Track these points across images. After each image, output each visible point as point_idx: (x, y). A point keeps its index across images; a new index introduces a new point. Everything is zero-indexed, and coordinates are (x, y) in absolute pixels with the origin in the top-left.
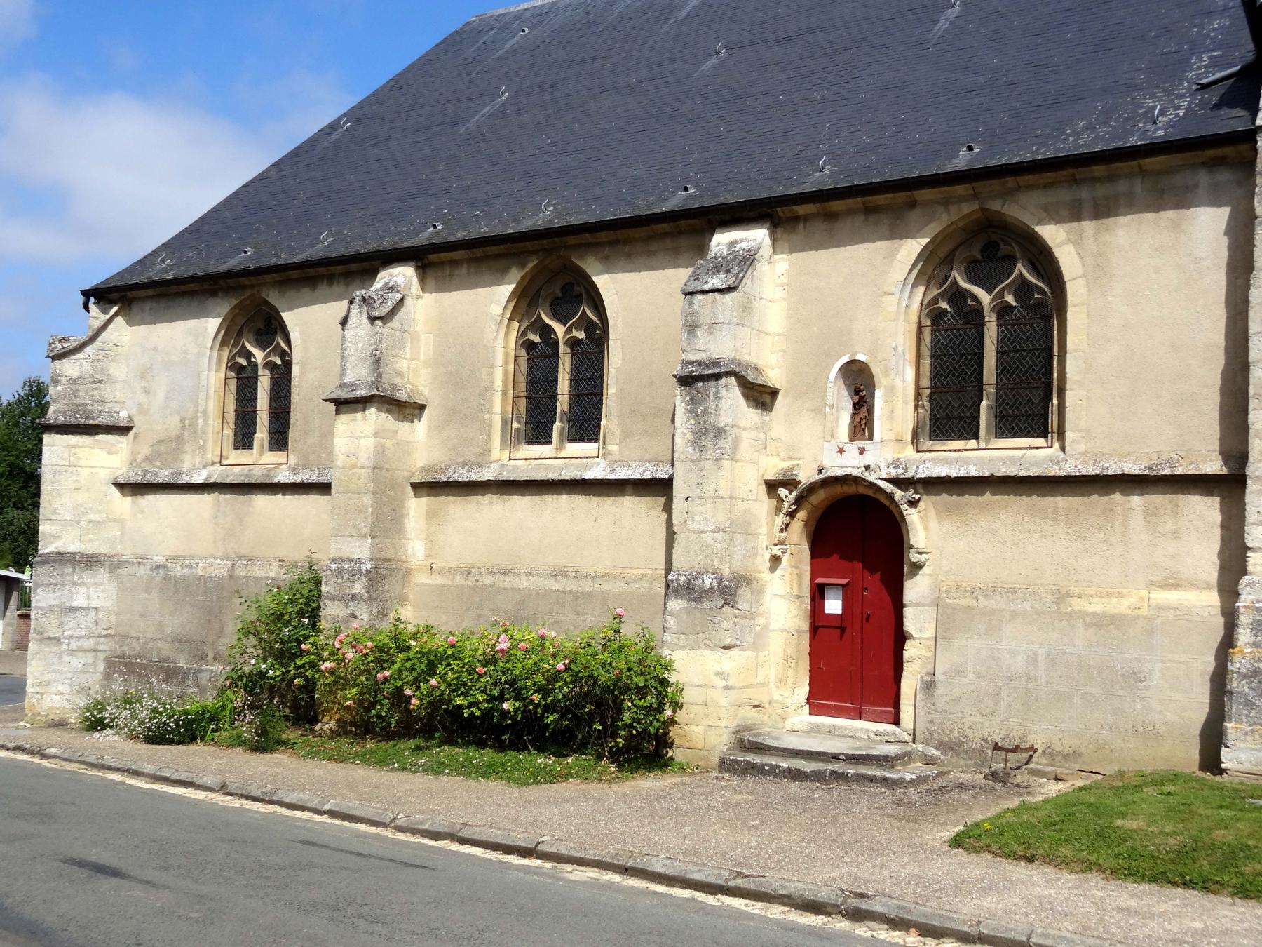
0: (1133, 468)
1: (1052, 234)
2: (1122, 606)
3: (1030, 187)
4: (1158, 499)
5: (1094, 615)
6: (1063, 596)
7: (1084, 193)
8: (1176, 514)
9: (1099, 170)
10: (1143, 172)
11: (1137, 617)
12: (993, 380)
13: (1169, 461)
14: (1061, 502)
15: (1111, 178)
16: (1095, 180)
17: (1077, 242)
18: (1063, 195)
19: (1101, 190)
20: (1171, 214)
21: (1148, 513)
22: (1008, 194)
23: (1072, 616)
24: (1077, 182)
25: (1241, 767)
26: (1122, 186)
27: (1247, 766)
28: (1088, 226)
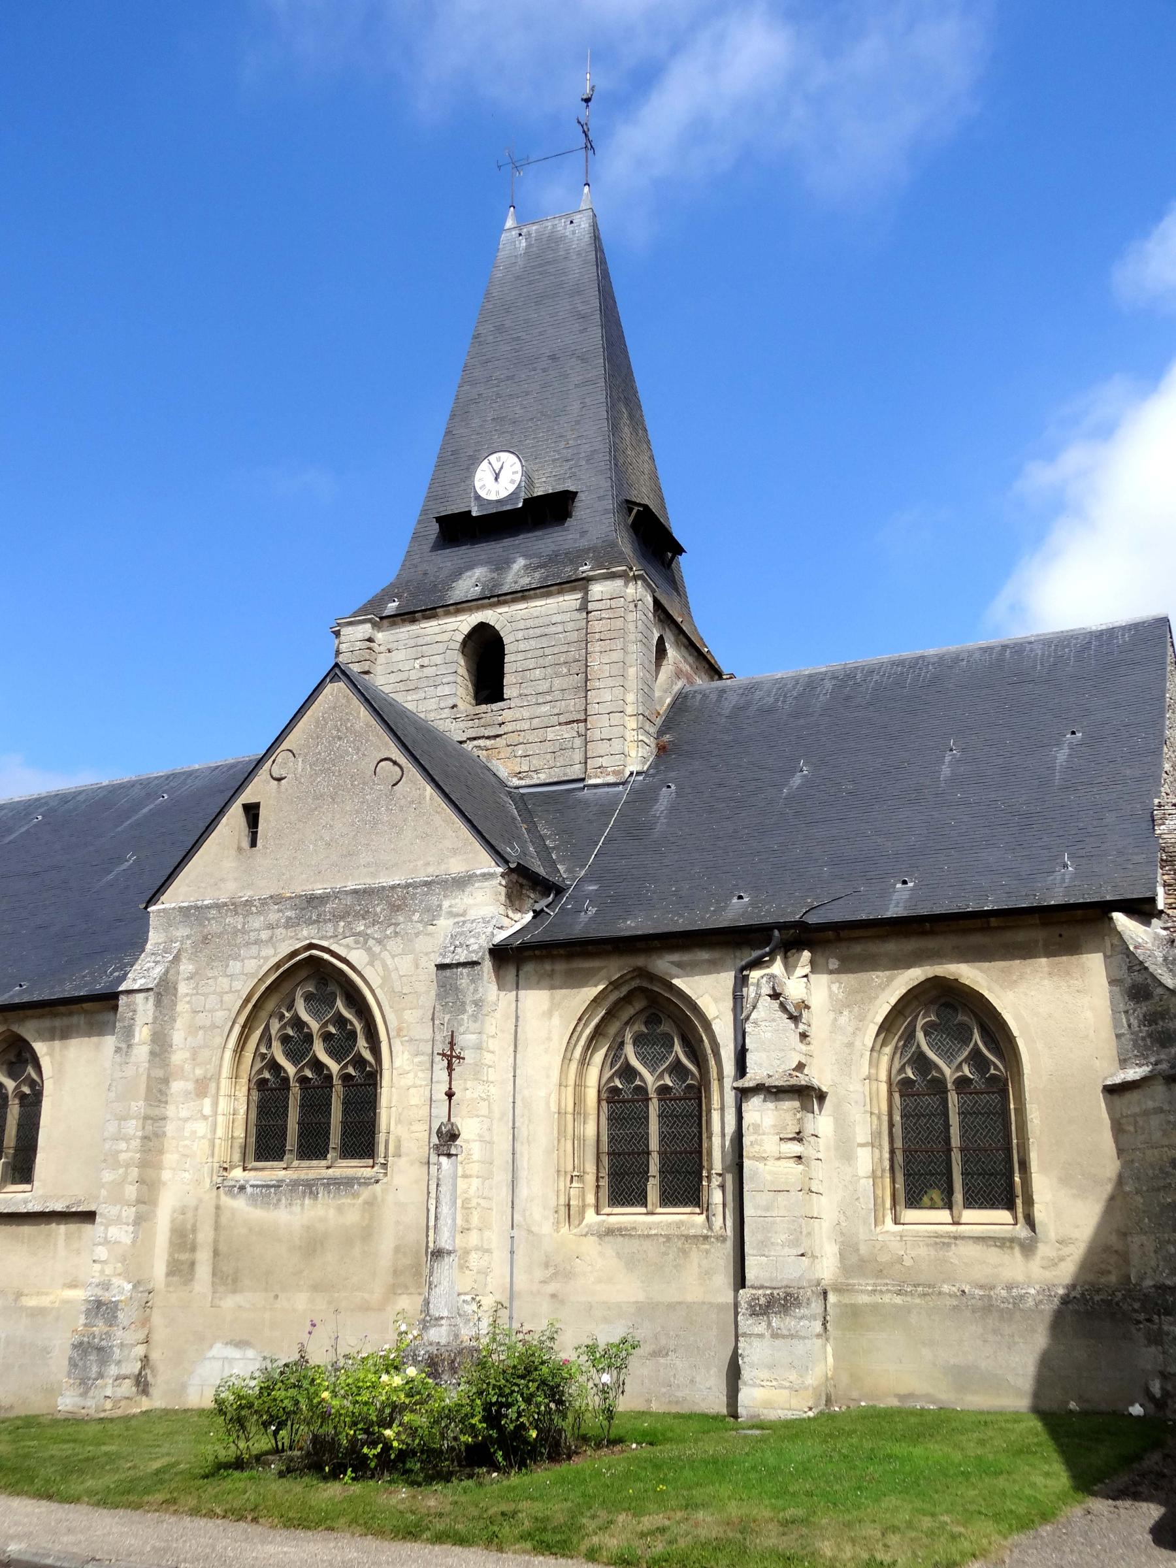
0: (59, 1207)
1: (40, 1047)
2: (45, 1301)
3: (32, 1017)
4: (73, 1227)
5: (32, 1308)
6: (19, 1295)
7: (58, 1023)
8: (80, 1238)
9: (62, 1009)
10: (85, 1012)
11: (52, 1309)
12: (13, 1143)
13: (79, 1203)
14: (27, 1230)
15: (71, 1014)
16: (63, 1015)
17: (51, 1054)
18: (47, 1023)
19: (66, 1021)
20: (95, 1039)
21: (68, 1237)
22: (22, 1020)
23: (23, 1309)
24: (55, 1015)
25: (66, 1409)
26: (75, 1020)
27: (69, 1408)
28: (57, 1043)
